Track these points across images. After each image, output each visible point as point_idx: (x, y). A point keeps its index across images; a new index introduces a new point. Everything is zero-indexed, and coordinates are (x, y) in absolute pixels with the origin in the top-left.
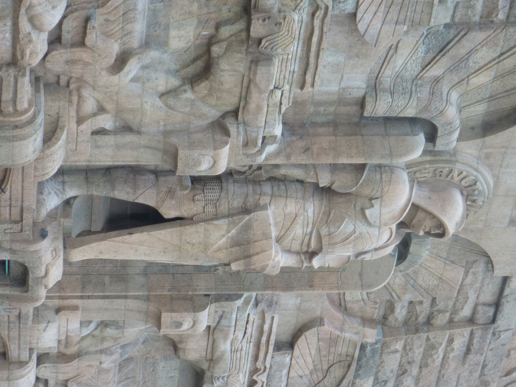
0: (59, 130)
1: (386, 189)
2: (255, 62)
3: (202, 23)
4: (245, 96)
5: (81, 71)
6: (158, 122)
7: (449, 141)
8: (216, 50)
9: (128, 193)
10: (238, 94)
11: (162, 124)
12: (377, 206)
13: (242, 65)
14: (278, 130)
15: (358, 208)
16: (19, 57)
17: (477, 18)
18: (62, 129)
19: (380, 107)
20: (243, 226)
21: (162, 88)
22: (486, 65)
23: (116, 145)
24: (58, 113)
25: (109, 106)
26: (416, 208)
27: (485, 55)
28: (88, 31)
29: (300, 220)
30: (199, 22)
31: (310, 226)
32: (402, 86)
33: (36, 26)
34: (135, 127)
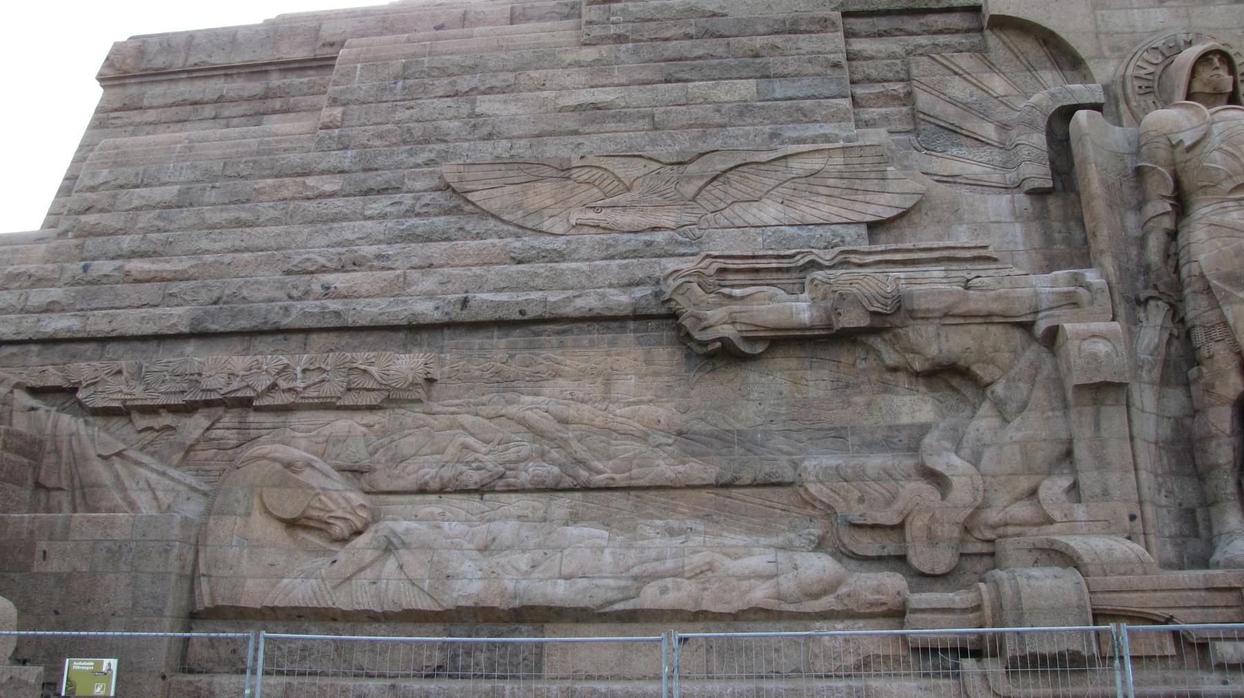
0: (1055, 547)
1: (1153, 134)
2: (912, 314)
3: (886, 388)
4: (987, 318)
5: (946, 526)
6: (1049, 418)
7: (1080, 91)
8: (917, 366)
9: (1219, 445)
10: (983, 328)
11: (1050, 414)
12: (1181, 136)
13: (923, 328)
15: (1188, 156)
16: (884, 608)
17: (905, 109)
18: (1053, 542)
19: (1037, 172)
20: (1231, 285)
21: (996, 422)
22: (974, 84)
23: (1098, 468)
24: (1030, 551)
25: (1025, 483)
26: (1189, 96)
27: (958, 88)
28: (870, 522)
29: (1216, 219)
30: (886, 391)
31: (1226, 204)
33: (830, 588)
34: (1062, 448)
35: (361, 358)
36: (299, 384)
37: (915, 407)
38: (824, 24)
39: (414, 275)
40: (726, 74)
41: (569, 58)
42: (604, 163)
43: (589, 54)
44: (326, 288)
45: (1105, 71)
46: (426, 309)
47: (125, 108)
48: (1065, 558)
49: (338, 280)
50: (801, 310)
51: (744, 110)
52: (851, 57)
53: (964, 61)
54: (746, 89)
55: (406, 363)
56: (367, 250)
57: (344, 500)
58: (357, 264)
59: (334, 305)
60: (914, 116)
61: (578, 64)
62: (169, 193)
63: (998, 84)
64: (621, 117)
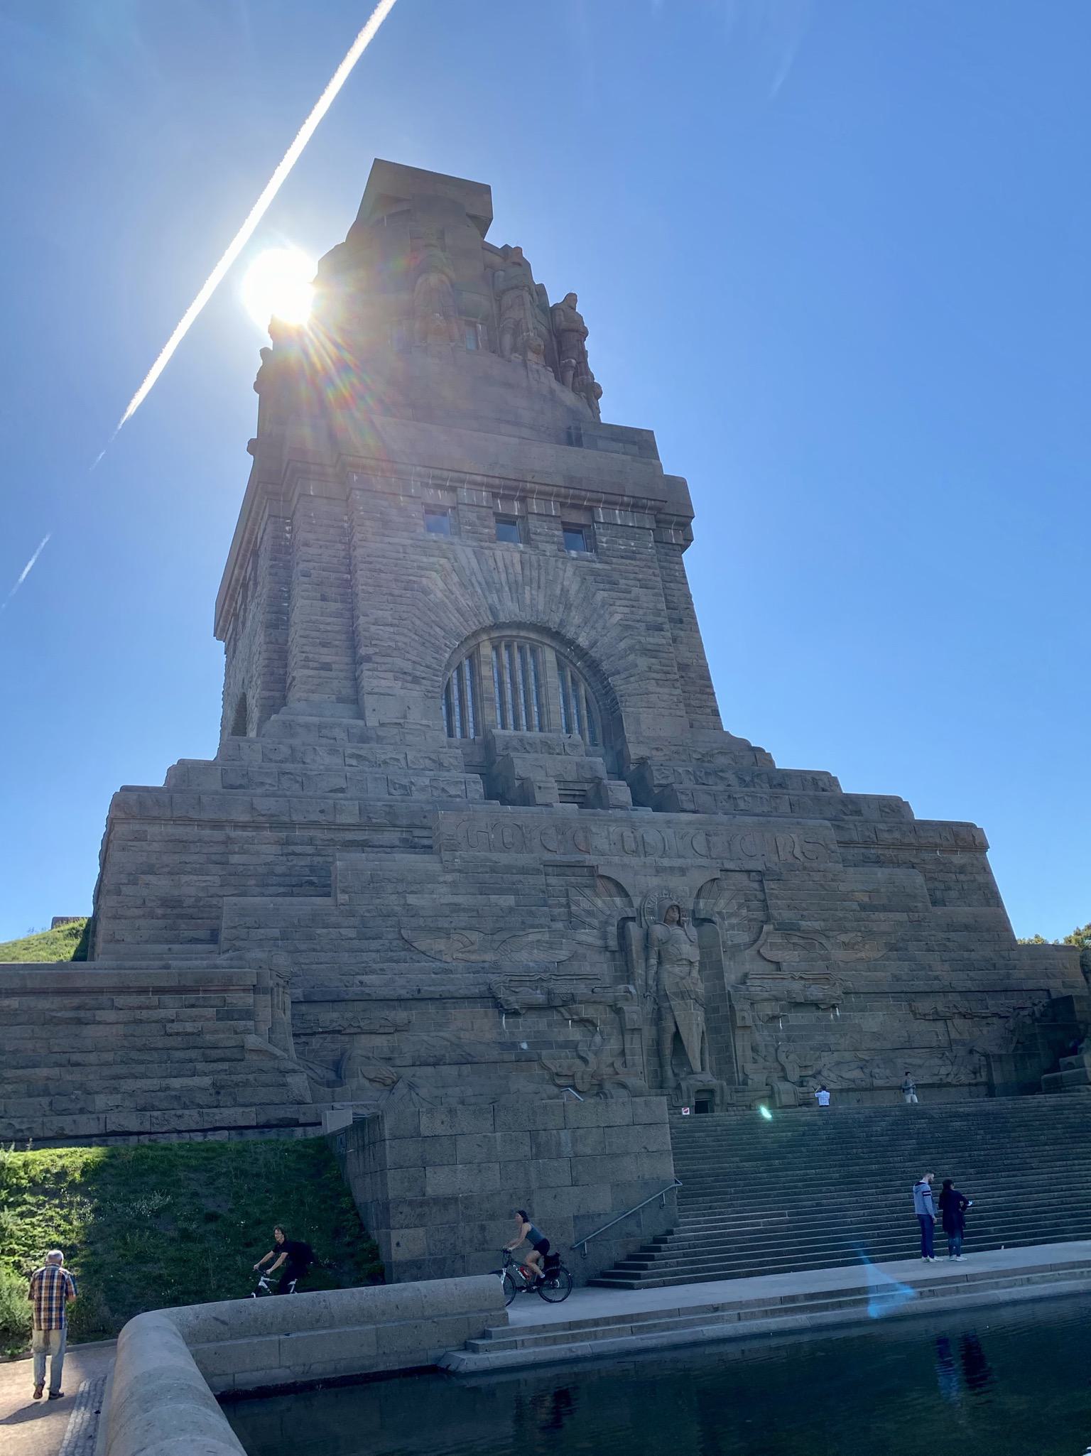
19: (613, 943)
32: (604, 937)
35: (385, 1013)
36: (362, 1024)
38: (538, 872)
39: (397, 978)
40: (501, 892)
41: (441, 879)
42: (464, 932)
43: (449, 878)
44: (361, 983)
45: (637, 902)
46: (403, 993)
47: (136, 839)
49: (365, 978)
50: (540, 997)
51: (511, 910)
52: (547, 885)
53: (588, 892)
54: (510, 900)
57: (386, 1071)
58: (373, 972)
59: (367, 990)
60: (570, 913)
61: (445, 882)
62: (276, 933)
63: (599, 903)
64: (464, 910)
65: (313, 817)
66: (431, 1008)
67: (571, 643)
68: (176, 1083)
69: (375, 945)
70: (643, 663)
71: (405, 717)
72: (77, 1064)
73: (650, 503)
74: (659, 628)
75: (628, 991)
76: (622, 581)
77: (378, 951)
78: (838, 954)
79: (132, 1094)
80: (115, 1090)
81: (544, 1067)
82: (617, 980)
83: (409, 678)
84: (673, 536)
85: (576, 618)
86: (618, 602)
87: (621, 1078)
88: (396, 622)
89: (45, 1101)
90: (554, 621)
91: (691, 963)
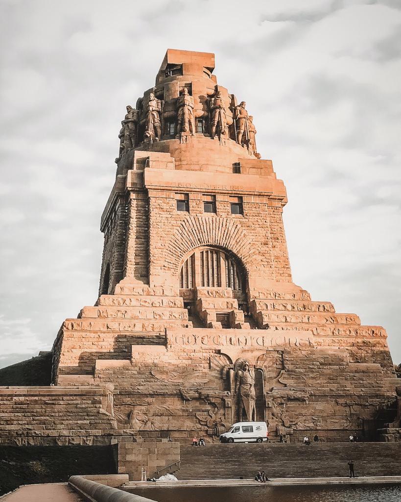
14: (226, 392)
37: (209, 407)
48: (223, 425)
50: (197, 395)
55: (150, 400)
56: (142, 383)
65: (126, 329)
66: (160, 398)
67: (231, 251)
68: (79, 422)
69: (143, 376)
70: (260, 258)
71: (164, 283)
72: (53, 416)
73: (266, 194)
74: (266, 244)
75: (228, 393)
76: (253, 226)
77: (144, 378)
78: (310, 382)
79: (67, 425)
80: (62, 424)
81: (197, 418)
82: (225, 390)
83: (167, 269)
84: (277, 204)
85: (233, 242)
86: (250, 234)
87: (223, 423)
88: (163, 247)
89: (44, 426)
90: (222, 243)
91: (251, 385)
